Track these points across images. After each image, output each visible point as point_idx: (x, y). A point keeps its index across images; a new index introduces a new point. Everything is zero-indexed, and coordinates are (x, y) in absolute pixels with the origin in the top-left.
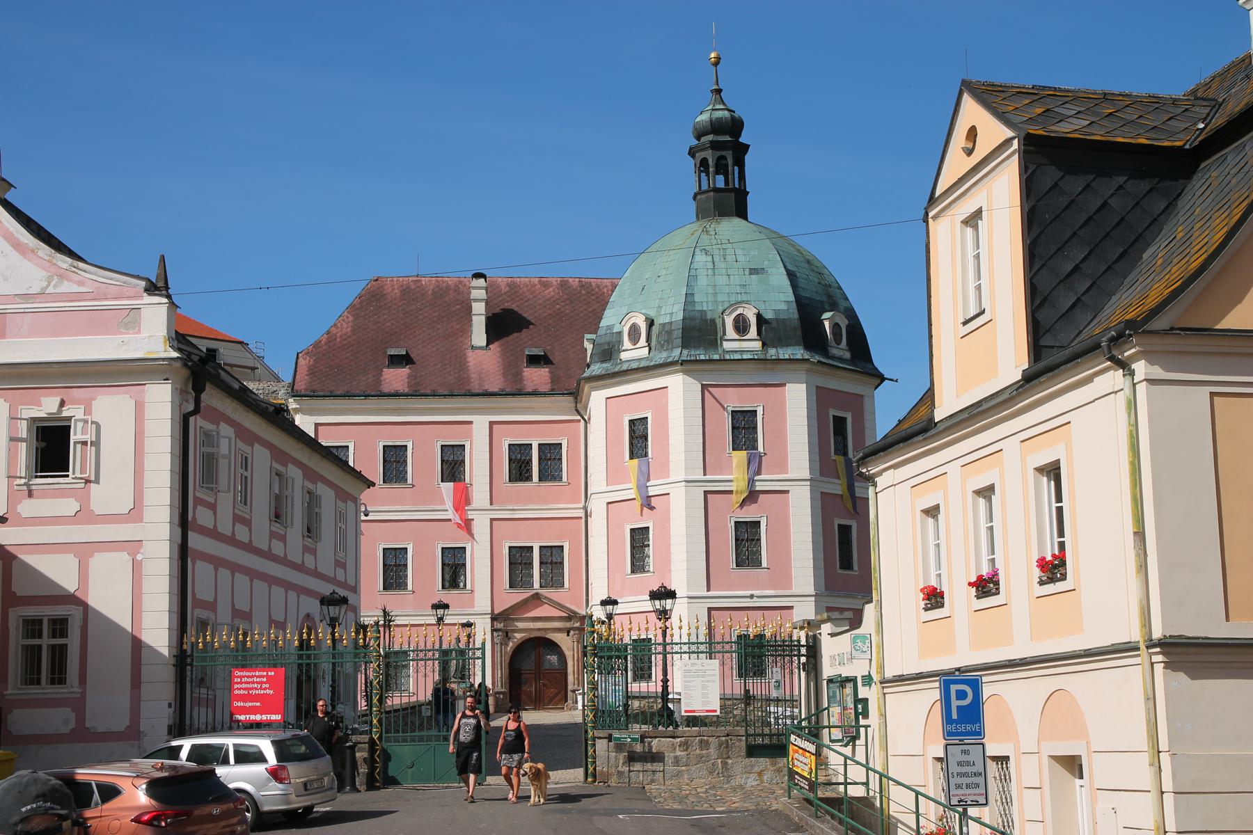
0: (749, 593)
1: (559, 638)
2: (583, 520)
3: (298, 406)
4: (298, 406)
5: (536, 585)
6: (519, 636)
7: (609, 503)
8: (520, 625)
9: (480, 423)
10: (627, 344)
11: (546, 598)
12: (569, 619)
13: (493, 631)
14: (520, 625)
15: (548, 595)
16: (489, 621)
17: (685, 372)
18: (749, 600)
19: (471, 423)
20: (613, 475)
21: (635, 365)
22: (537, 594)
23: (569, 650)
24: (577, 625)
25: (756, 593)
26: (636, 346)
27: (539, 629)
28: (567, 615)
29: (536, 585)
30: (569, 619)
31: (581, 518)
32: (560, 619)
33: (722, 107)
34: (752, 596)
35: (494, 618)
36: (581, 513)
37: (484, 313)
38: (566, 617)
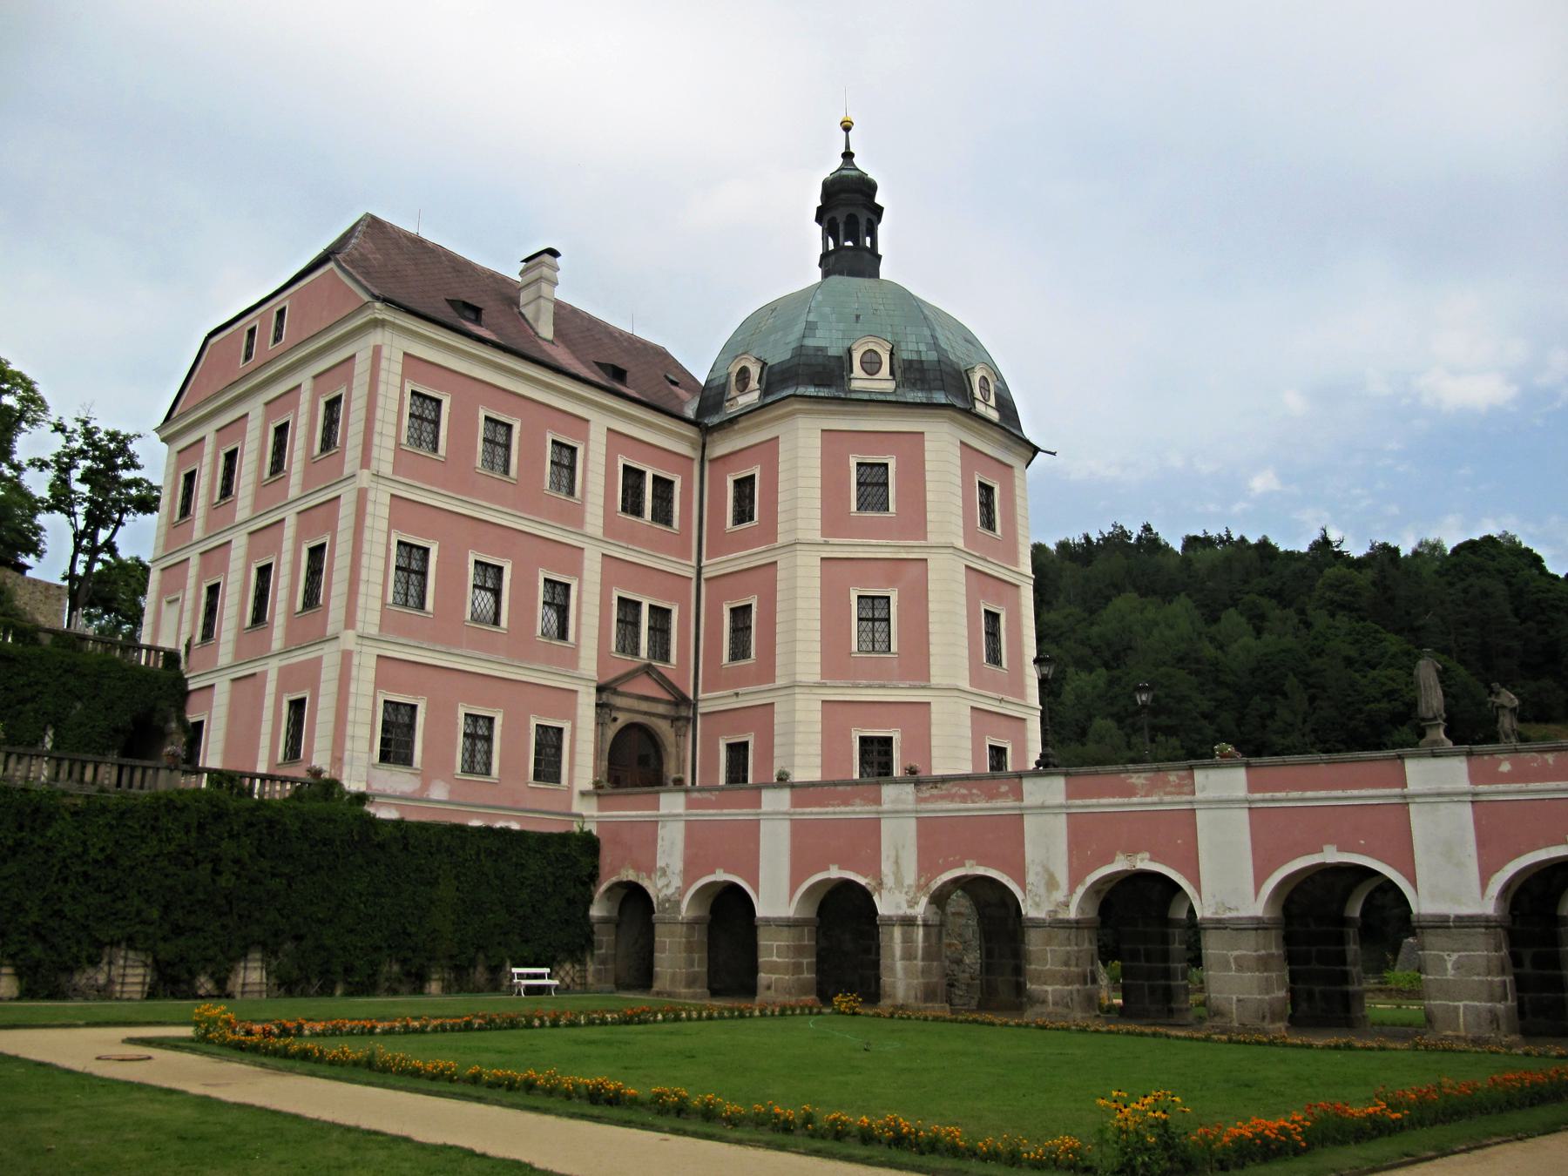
0: (1001, 696)
1: (664, 728)
6: (623, 719)
9: (599, 425)
10: (857, 371)
13: (597, 705)
15: (660, 669)
16: (593, 691)
18: (997, 703)
20: (834, 523)
22: (649, 666)
25: (1007, 698)
27: (646, 713)
31: (691, 579)
32: (668, 702)
35: (600, 689)
36: (692, 574)
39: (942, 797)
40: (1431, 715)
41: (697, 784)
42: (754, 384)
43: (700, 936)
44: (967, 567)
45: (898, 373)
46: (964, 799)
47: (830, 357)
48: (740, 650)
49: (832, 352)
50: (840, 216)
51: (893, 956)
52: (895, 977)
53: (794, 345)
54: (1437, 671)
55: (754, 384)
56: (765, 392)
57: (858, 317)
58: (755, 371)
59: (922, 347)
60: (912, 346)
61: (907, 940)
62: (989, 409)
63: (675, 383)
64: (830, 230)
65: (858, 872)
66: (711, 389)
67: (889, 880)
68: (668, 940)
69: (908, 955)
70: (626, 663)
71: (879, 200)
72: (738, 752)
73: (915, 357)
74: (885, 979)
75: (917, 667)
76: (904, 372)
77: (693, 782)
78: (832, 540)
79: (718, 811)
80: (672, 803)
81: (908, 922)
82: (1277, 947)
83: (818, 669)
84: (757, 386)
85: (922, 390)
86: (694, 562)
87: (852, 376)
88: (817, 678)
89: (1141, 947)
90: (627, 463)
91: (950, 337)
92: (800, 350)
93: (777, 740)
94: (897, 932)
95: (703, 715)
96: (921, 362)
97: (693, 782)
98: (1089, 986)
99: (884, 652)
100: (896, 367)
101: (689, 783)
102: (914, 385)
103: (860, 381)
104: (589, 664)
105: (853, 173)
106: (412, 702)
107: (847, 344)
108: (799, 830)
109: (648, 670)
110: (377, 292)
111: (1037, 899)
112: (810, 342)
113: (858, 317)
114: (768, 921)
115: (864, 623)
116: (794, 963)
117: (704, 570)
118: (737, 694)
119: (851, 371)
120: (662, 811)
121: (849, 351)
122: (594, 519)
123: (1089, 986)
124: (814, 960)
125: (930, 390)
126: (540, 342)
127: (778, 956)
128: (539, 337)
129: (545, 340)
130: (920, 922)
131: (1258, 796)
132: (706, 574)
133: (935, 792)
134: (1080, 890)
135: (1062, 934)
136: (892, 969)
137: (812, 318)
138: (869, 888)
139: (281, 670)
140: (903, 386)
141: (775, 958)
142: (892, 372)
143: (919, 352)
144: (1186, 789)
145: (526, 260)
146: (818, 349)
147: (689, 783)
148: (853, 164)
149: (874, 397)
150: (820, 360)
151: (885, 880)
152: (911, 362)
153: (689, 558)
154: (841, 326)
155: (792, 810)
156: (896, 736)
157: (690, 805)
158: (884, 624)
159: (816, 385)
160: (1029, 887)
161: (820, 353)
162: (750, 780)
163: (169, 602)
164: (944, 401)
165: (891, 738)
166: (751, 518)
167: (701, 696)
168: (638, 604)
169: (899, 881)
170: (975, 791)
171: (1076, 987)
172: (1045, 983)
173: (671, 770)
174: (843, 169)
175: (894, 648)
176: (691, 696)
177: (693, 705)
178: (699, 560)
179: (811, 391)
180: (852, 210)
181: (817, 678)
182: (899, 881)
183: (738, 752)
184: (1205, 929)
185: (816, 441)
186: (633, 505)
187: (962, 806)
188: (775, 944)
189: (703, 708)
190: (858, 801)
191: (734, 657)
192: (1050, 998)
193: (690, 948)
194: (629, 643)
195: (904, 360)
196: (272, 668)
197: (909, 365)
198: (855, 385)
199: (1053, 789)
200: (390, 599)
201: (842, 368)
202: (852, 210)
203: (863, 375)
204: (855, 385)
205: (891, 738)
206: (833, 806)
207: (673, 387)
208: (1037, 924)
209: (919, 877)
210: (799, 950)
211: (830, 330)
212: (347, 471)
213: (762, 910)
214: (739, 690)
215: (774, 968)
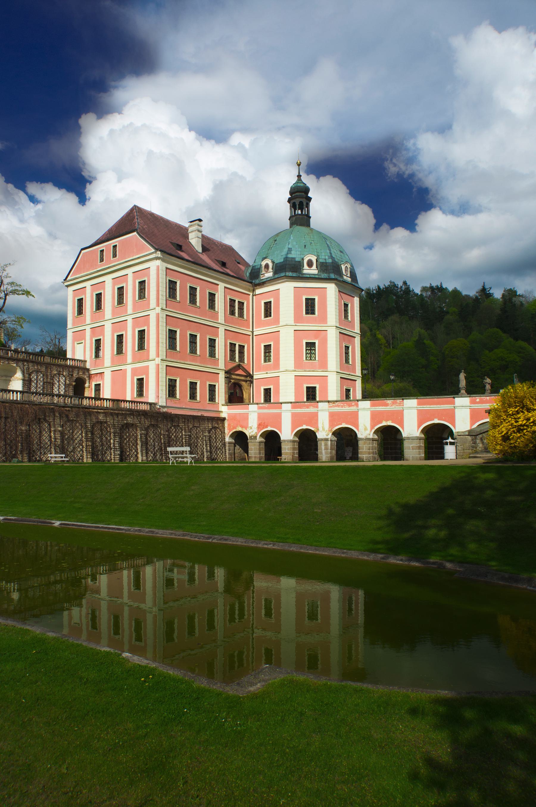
0: (348, 373)
1: (243, 383)
2: (251, 337)
3: (162, 257)
4: (162, 257)
5: (237, 360)
6: (232, 381)
7: (294, 330)
8: (233, 377)
9: (221, 286)
10: (306, 266)
11: (242, 366)
12: (246, 376)
13: (225, 377)
14: (233, 377)
16: (224, 373)
17: (336, 284)
18: (348, 376)
19: (218, 285)
20: (298, 319)
21: (308, 276)
22: (240, 364)
23: (247, 389)
24: (250, 379)
26: (311, 269)
28: (246, 374)
29: (237, 360)
30: (246, 376)
31: (250, 335)
33: (301, 182)
34: (349, 375)
35: (225, 373)
36: (250, 333)
37: (201, 237)
38: (245, 375)
39: (336, 406)
40: (462, 387)
41: (254, 402)
42: (270, 269)
43: (263, 446)
44: (340, 333)
45: (319, 267)
46: (342, 406)
47: (296, 261)
48: (267, 358)
49: (297, 260)
50: (297, 201)
51: (322, 450)
52: (322, 454)
53: (284, 257)
54: (465, 376)
55: (270, 269)
56: (275, 273)
57: (305, 246)
58: (271, 265)
59: (327, 257)
60: (323, 257)
61: (326, 445)
62: (348, 278)
63: (239, 263)
64: (293, 206)
65: (311, 427)
66: (255, 269)
67: (320, 428)
68: (253, 447)
69: (326, 449)
70: (232, 365)
71: (310, 195)
72: (267, 392)
73: (324, 261)
74: (319, 455)
75: (324, 365)
76: (321, 267)
77: (253, 401)
78: (297, 324)
79: (268, 410)
80: (253, 408)
81: (326, 440)
82: (422, 444)
83: (293, 366)
84: (272, 271)
85: (326, 273)
86: (251, 330)
87: (304, 268)
88: (293, 369)
89: (389, 446)
90: (231, 298)
91: (336, 252)
92: (286, 259)
93: (281, 388)
94: (323, 443)
95: (255, 379)
96: (326, 263)
97: (253, 401)
98: (375, 455)
99: (314, 360)
100: (318, 264)
101: (251, 402)
102: (324, 271)
103: (307, 270)
104: (222, 365)
105: (302, 185)
106: (176, 379)
107: (302, 256)
108: (294, 415)
109: (239, 367)
110: (157, 247)
111: (362, 433)
112: (290, 256)
113: (305, 246)
114: (285, 441)
115: (307, 351)
116: (293, 452)
117: (254, 332)
118: (267, 373)
119: (303, 267)
120: (249, 410)
121: (303, 259)
122: (221, 318)
123: (375, 455)
124: (298, 451)
125: (329, 273)
126: (198, 254)
127: (288, 450)
128: (198, 252)
129: (199, 253)
130: (329, 440)
131: (419, 406)
132: (255, 333)
133: (334, 405)
134: (373, 431)
135: (368, 441)
136: (321, 453)
137: (290, 247)
138: (315, 431)
139: (132, 369)
140: (320, 272)
141: (287, 451)
142: (317, 267)
143: (325, 259)
144: (401, 405)
145: (191, 222)
146: (292, 258)
147: (251, 402)
148: (301, 180)
149: (311, 276)
150: (293, 263)
151: (319, 429)
152: (323, 263)
153: (249, 328)
154: (300, 250)
155: (292, 410)
156: (317, 386)
157: (259, 408)
158: (314, 351)
159: (292, 272)
160: (359, 430)
161: (293, 260)
162: (272, 401)
163: (78, 344)
164: (334, 277)
165: (316, 387)
166: (270, 316)
167: (254, 374)
168: (235, 344)
169: (323, 429)
170: (345, 405)
171: (372, 455)
172: (364, 455)
173: (245, 396)
174: (298, 183)
175: (317, 359)
176: (251, 373)
177: (253, 377)
178: (253, 329)
179: (290, 274)
180: (301, 200)
181: (293, 369)
182: (323, 429)
183: (267, 392)
184: (404, 440)
185: (292, 291)
186: (232, 313)
187: (342, 409)
188: (287, 447)
189: (255, 377)
190: (311, 407)
191: (265, 361)
192: (365, 458)
193: (260, 450)
194: (232, 358)
195: (321, 262)
196: (129, 368)
197: (322, 263)
198: (305, 272)
199: (367, 404)
200: (168, 348)
201: (300, 265)
202: (301, 200)
203: (307, 268)
204: (305, 272)
205: (316, 387)
206: (304, 408)
207: (239, 265)
208: (362, 439)
209: (329, 428)
210: (294, 449)
211: (296, 251)
212: (151, 307)
213: (283, 438)
214: (268, 372)
215: (286, 454)
